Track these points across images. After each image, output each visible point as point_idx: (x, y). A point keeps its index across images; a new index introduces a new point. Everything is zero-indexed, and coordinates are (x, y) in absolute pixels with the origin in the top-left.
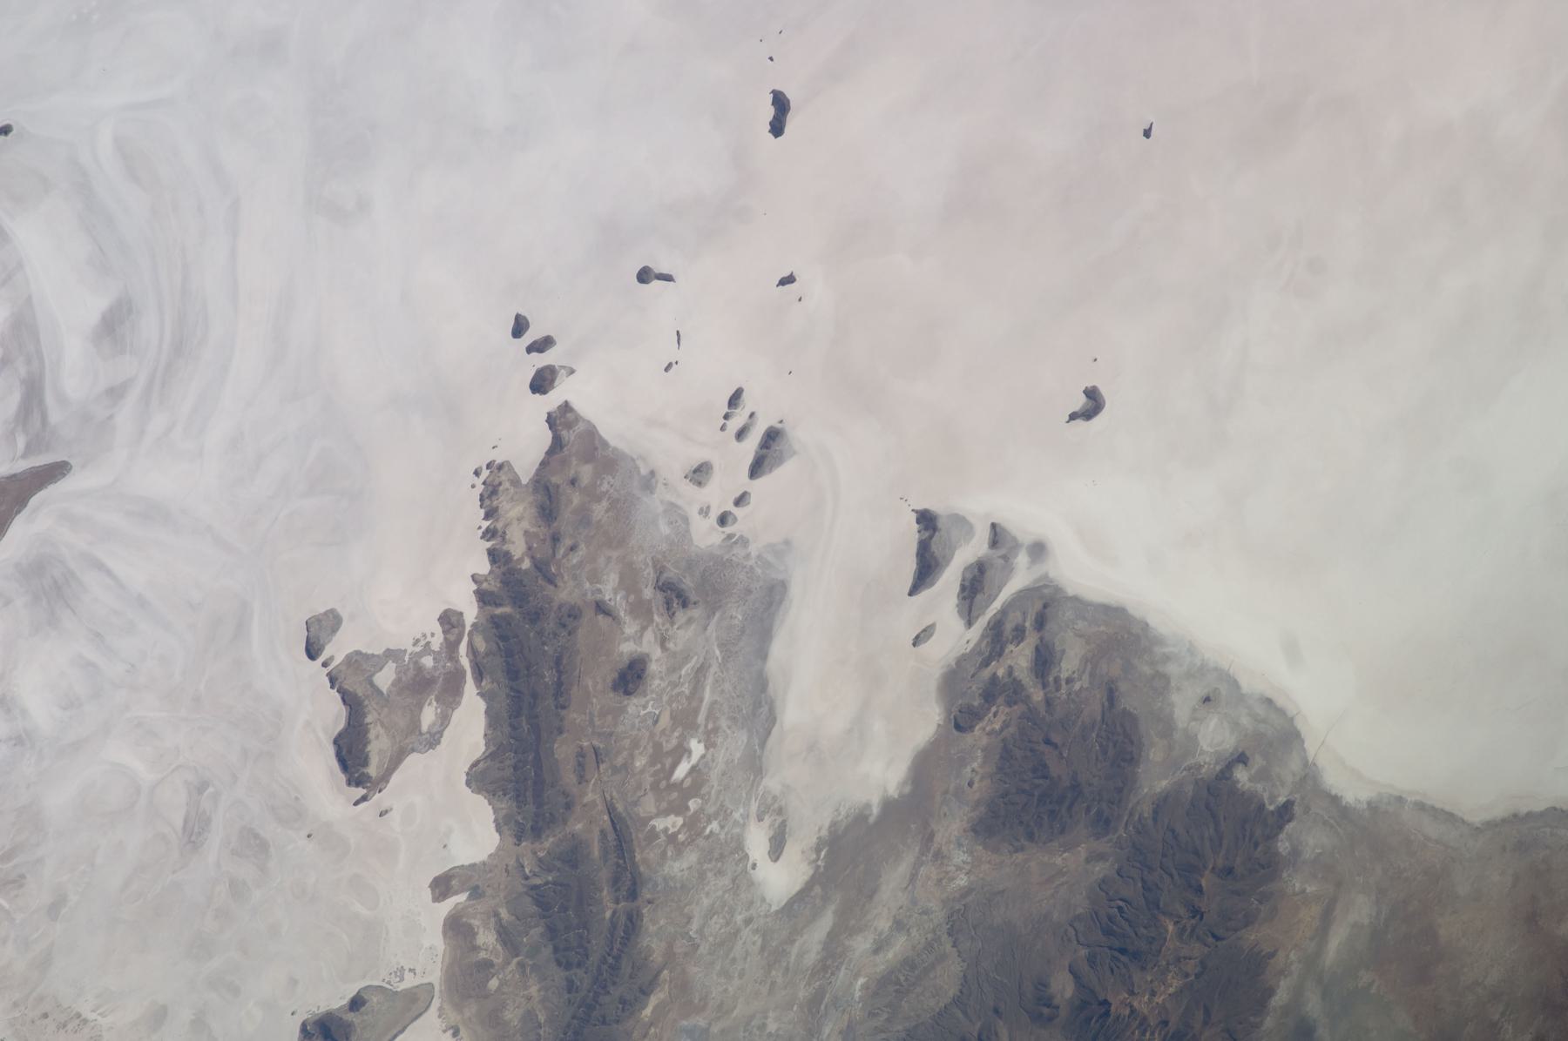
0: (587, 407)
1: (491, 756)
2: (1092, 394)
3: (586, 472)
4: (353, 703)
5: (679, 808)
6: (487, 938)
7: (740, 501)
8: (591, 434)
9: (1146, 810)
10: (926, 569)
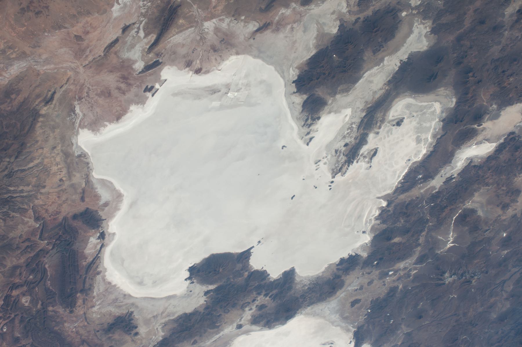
0: (329, 175)
1: (364, 145)
2: (283, 148)
3: (335, 170)
4: (371, 159)
5: (352, 127)
6: (378, 124)
7: (323, 158)
8: (332, 174)
9: (308, 94)
10: (311, 139)
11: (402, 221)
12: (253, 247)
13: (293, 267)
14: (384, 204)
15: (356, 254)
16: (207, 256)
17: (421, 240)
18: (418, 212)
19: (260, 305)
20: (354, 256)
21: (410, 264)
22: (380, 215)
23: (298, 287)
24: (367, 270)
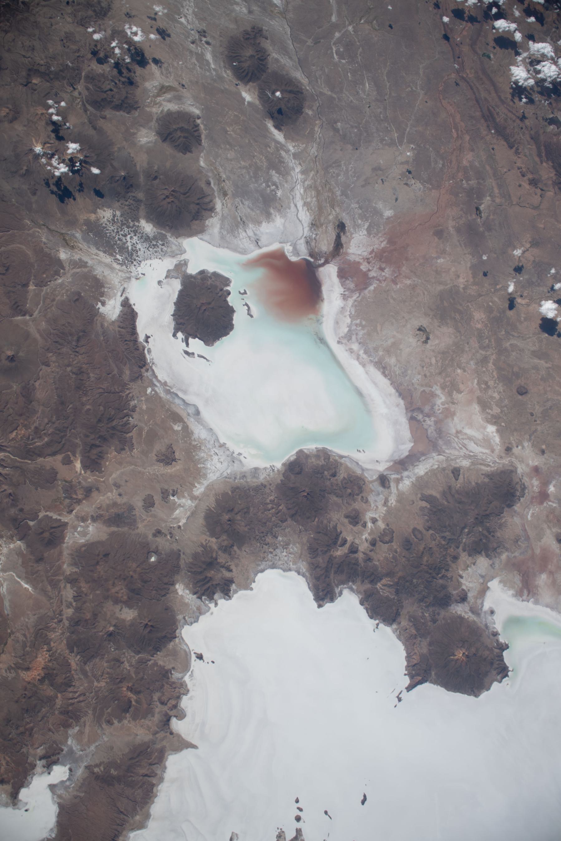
11: (127, 665)
12: (409, 688)
13: (320, 606)
14: (176, 725)
15: (200, 598)
16: (484, 695)
17: (69, 593)
18: (98, 681)
19: (359, 527)
20: (203, 594)
21: (75, 528)
22: (179, 698)
23: (295, 548)
24: (163, 543)
